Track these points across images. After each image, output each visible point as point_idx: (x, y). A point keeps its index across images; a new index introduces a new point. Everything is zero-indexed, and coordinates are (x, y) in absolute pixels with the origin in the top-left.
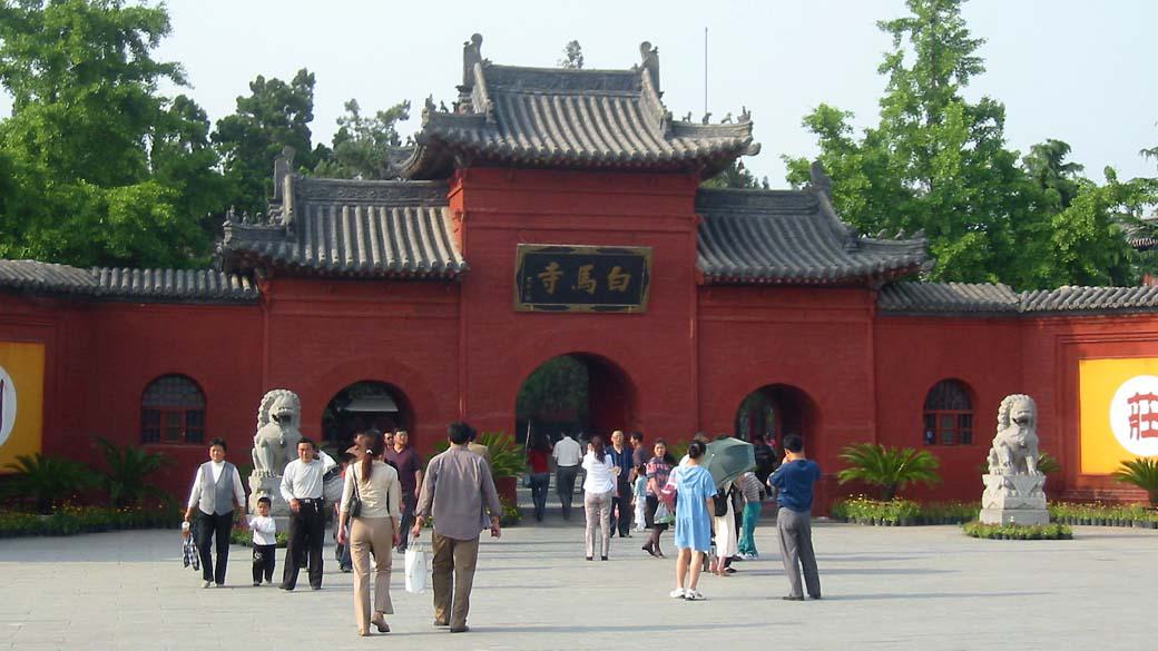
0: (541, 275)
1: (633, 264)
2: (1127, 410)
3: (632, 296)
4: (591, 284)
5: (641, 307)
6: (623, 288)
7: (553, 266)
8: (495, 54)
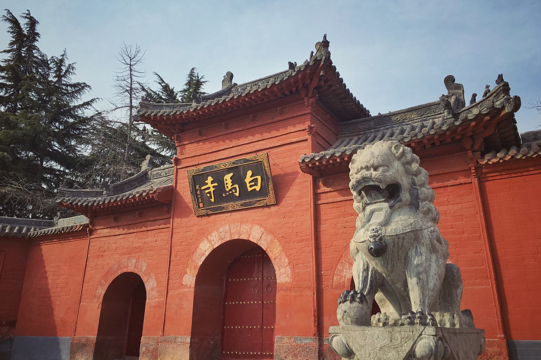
0: (203, 188)
1: (258, 168)
3: (263, 192)
4: (235, 188)
5: (271, 198)
7: (210, 179)
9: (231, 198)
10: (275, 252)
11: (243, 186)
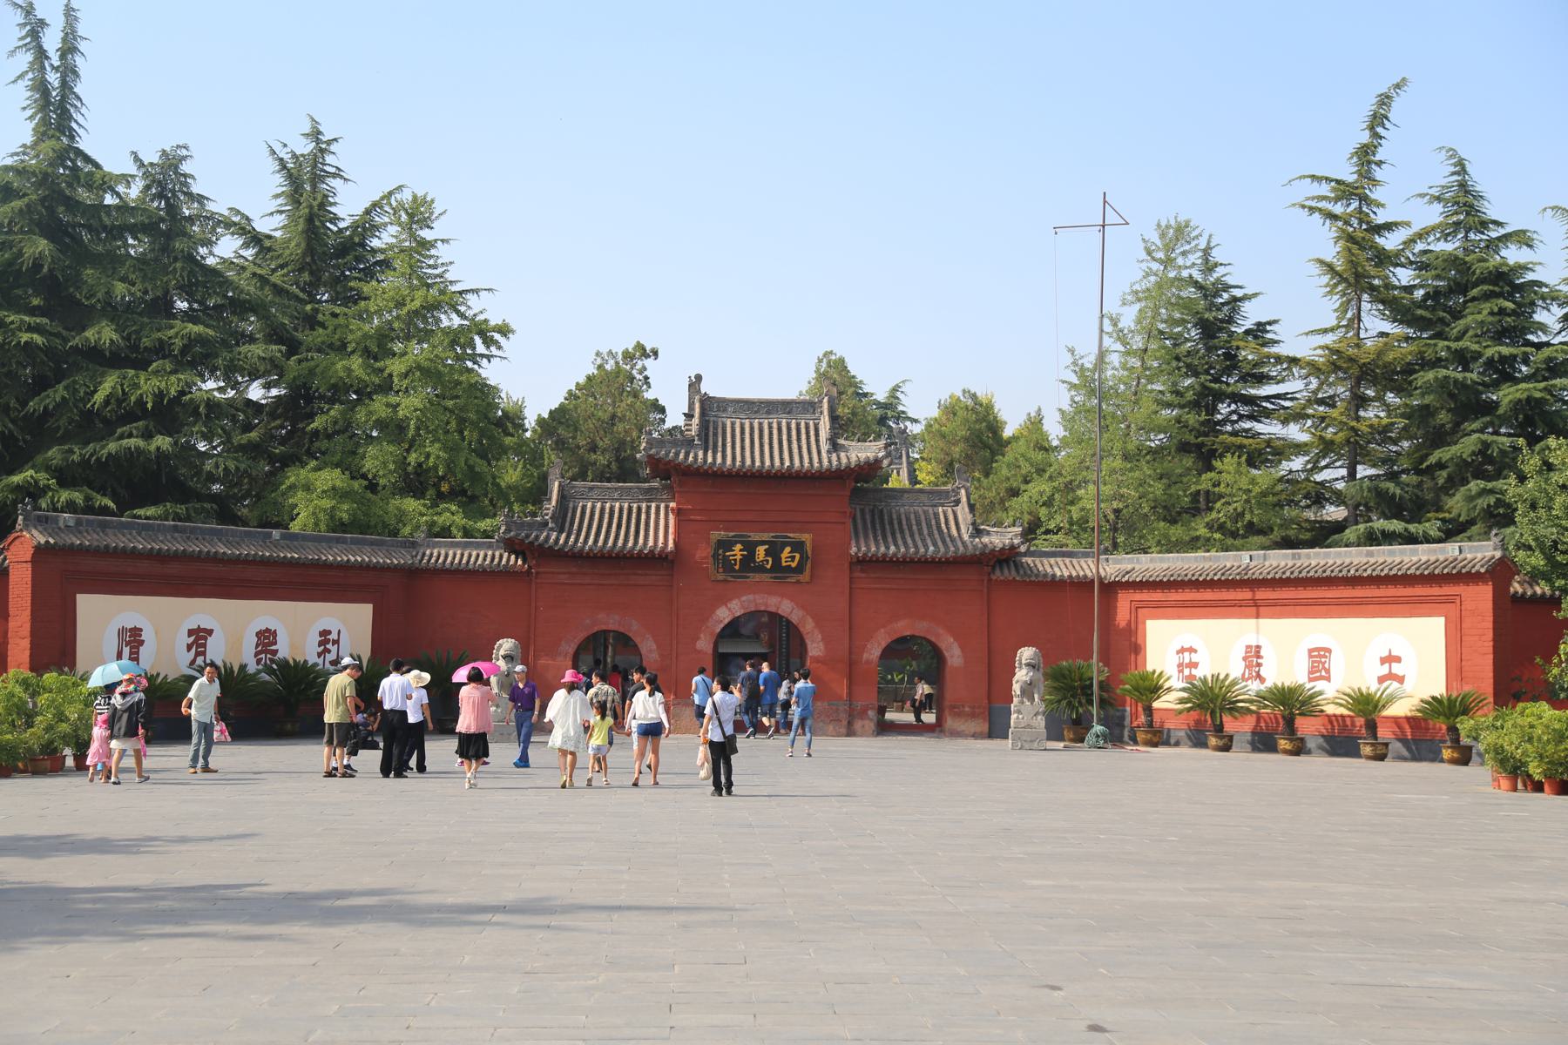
1: (798, 546)
2: (1175, 660)
3: (799, 569)
5: (805, 577)
6: (794, 565)
7: (739, 546)
8: (709, 388)
9: (761, 569)
10: (808, 627)
11: (777, 560)
